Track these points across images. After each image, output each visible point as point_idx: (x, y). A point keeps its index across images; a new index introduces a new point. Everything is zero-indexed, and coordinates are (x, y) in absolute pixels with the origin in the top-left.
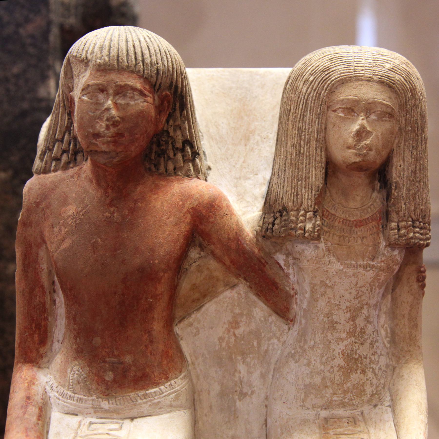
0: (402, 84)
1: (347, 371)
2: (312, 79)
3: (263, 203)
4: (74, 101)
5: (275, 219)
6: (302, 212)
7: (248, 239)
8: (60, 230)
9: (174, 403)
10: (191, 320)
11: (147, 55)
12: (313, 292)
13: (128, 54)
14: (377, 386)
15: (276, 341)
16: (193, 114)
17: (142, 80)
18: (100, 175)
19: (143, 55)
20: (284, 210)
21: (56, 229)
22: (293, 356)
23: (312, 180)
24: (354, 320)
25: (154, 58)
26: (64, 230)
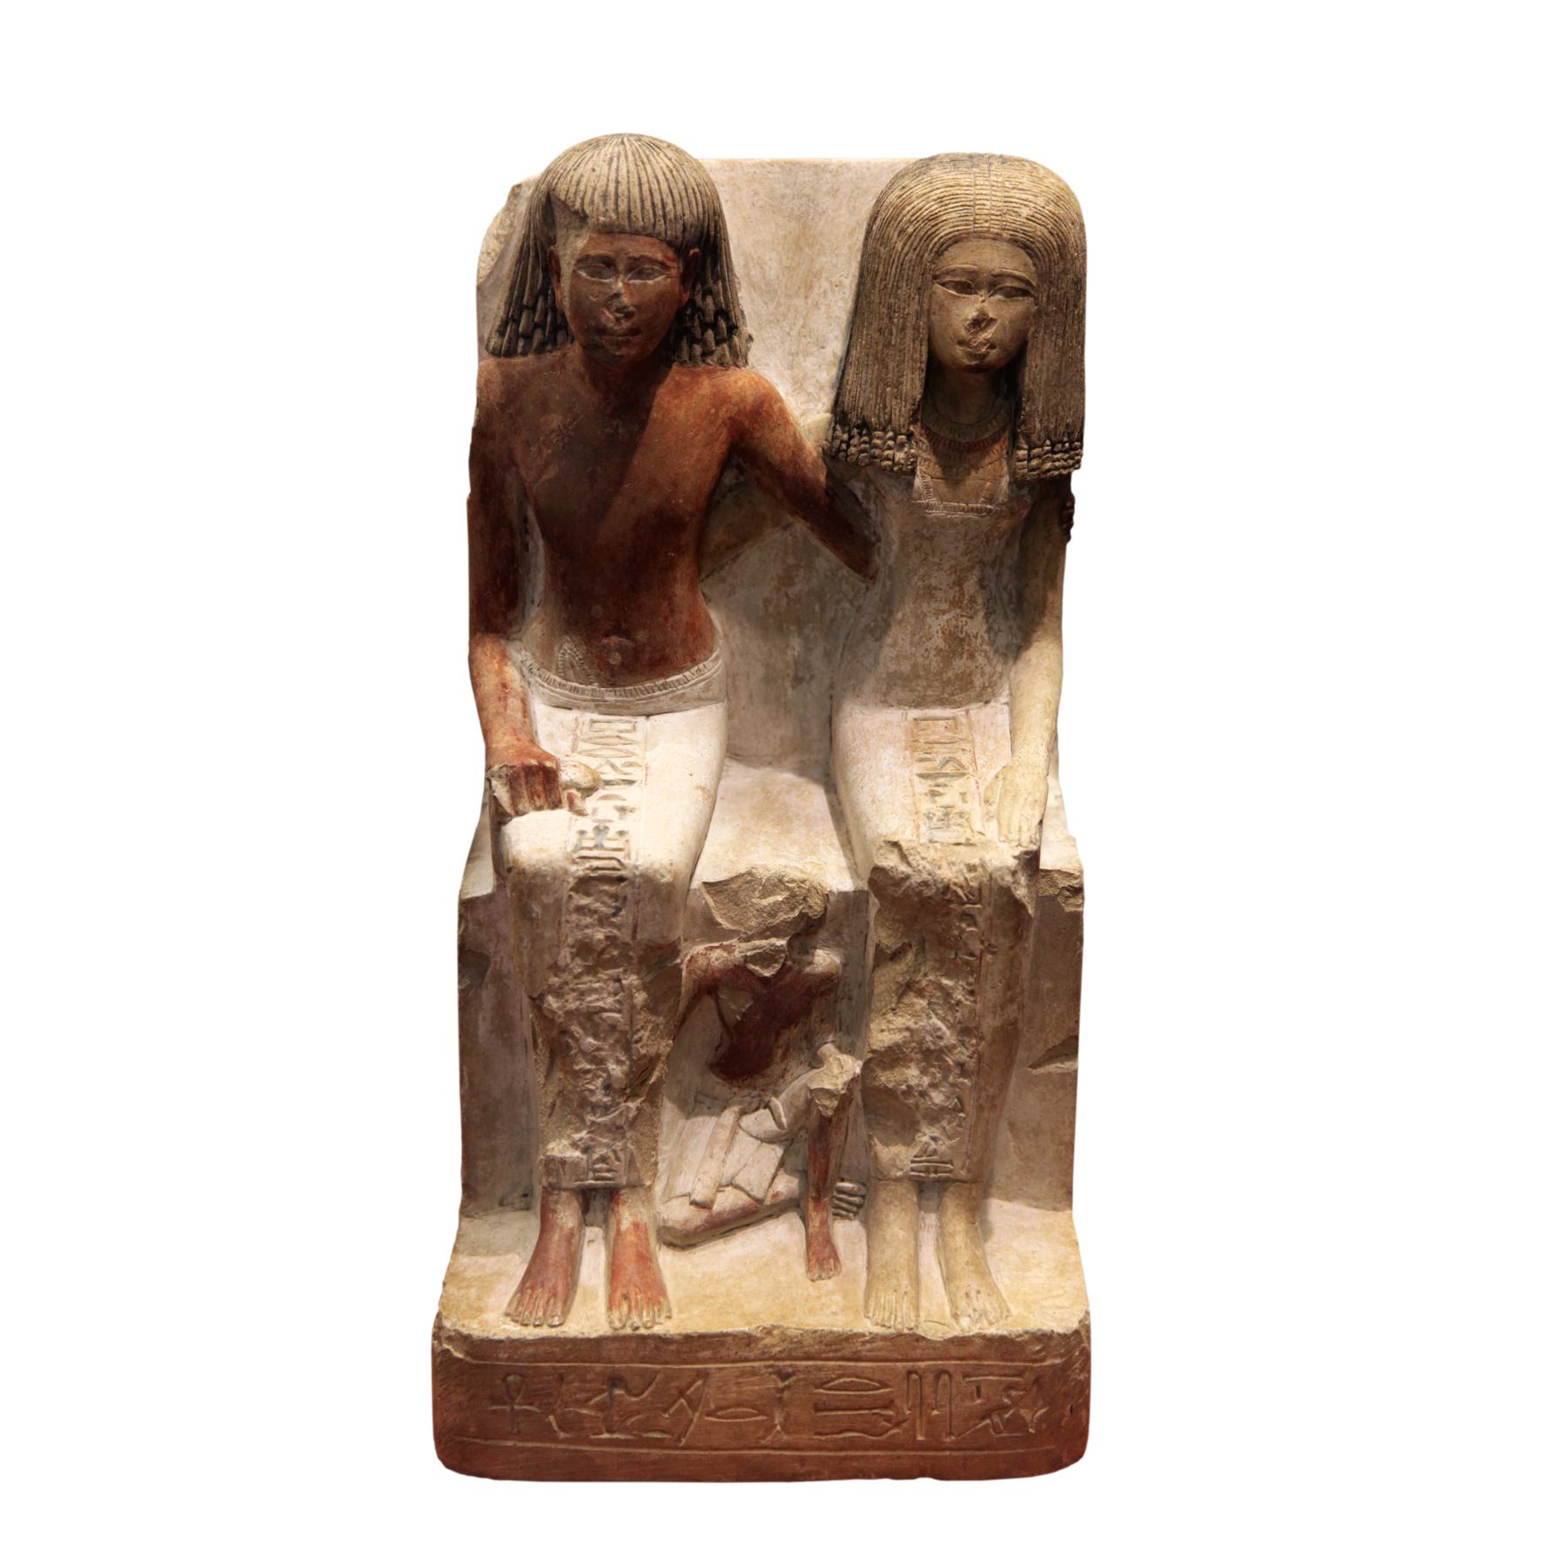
0: (1045, 241)
1: (948, 656)
2: (910, 230)
3: (832, 396)
4: (558, 262)
5: (851, 437)
6: (890, 434)
7: (810, 460)
8: (540, 449)
9: (703, 696)
10: (723, 573)
11: (670, 207)
12: (903, 543)
13: (643, 208)
14: (991, 676)
15: (847, 605)
16: (730, 269)
17: (664, 245)
18: (597, 368)
19: (664, 207)
20: (864, 426)
21: (534, 449)
22: (872, 631)
23: (906, 387)
24: (960, 585)
25: (679, 207)
26: (547, 452)
